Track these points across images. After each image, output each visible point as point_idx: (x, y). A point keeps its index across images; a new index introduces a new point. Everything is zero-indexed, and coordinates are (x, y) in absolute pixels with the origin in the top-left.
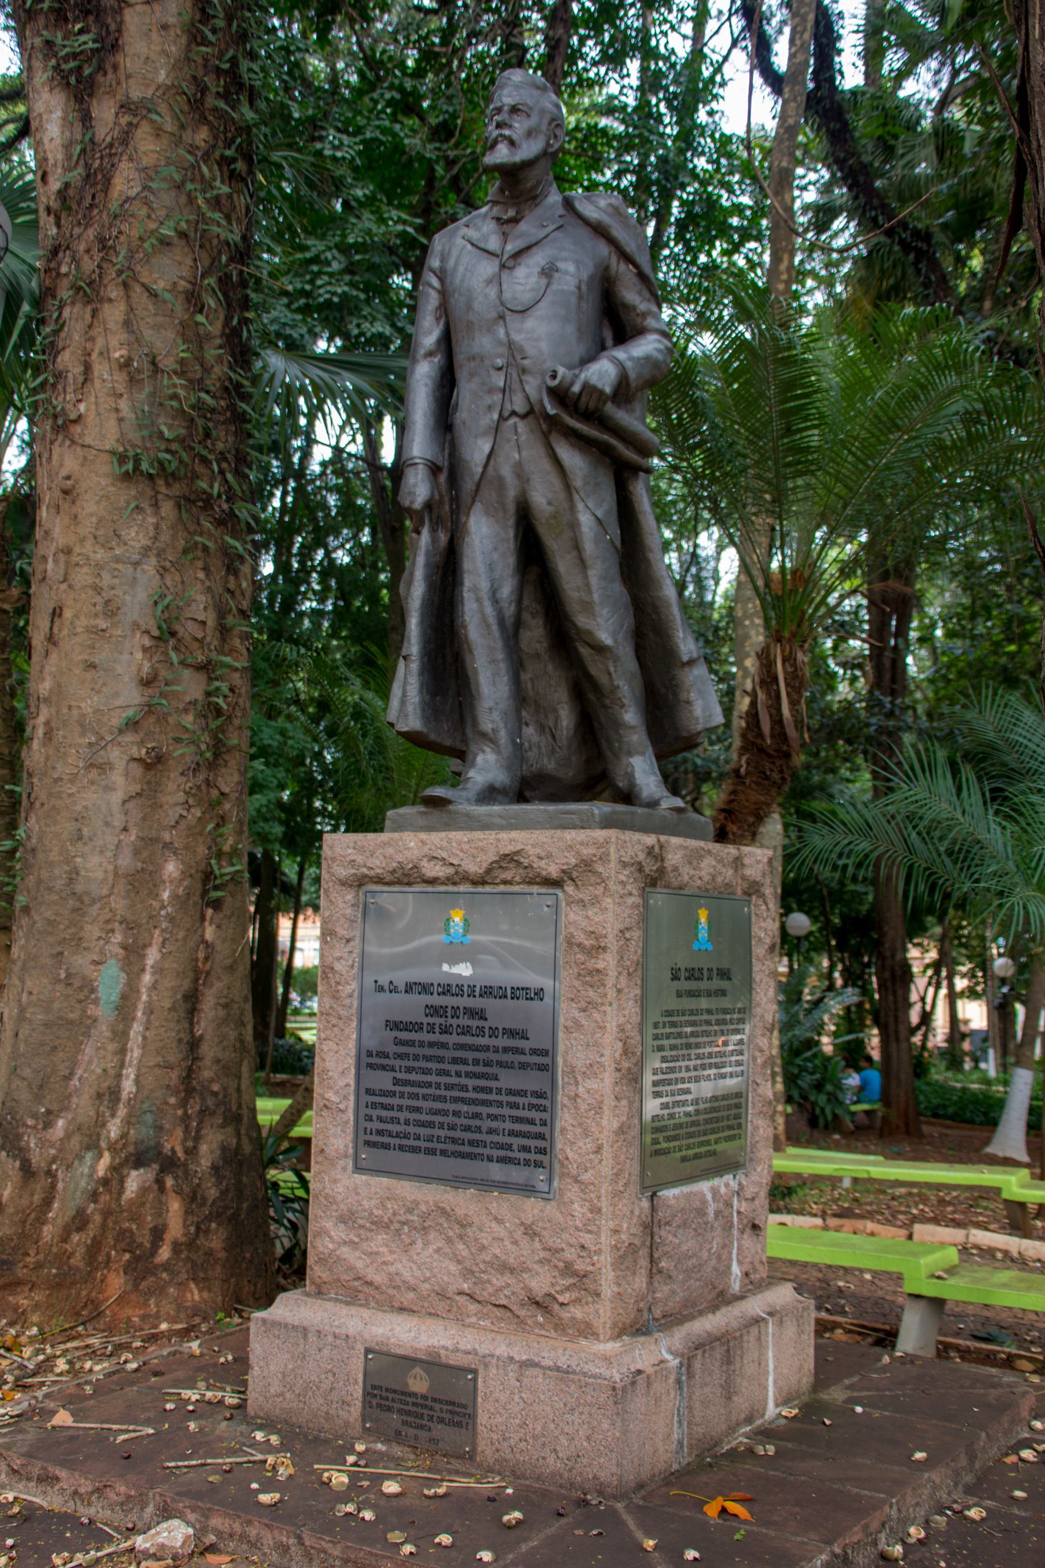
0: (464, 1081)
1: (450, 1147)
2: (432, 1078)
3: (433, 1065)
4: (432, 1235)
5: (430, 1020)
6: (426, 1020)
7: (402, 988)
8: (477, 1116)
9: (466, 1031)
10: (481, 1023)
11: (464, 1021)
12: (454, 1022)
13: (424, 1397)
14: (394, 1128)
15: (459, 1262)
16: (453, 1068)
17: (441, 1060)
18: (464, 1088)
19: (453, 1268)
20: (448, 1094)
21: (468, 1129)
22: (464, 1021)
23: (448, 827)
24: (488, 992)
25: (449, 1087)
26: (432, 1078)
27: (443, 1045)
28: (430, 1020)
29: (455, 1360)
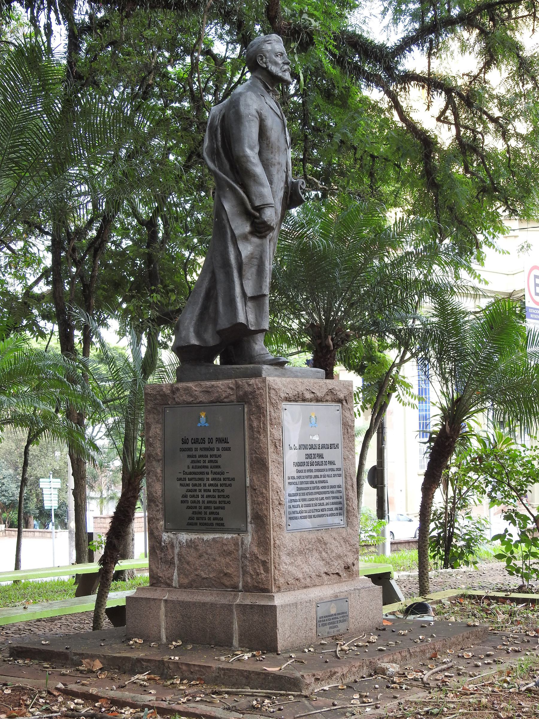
0: (318, 485)
1: (316, 513)
2: (309, 485)
3: (309, 480)
4: (314, 551)
5: (307, 460)
6: (306, 461)
7: (298, 447)
8: (322, 499)
9: (318, 464)
10: (322, 460)
11: (317, 460)
12: (314, 460)
13: (335, 615)
14: (298, 509)
15: (323, 560)
16: (314, 480)
17: (311, 477)
18: (318, 488)
19: (322, 563)
20: (314, 491)
21: (320, 505)
22: (317, 460)
23: (283, 375)
24: (324, 447)
25: (314, 488)
26: (309, 485)
27: (311, 471)
28: (307, 460)
29: (342, 596)
